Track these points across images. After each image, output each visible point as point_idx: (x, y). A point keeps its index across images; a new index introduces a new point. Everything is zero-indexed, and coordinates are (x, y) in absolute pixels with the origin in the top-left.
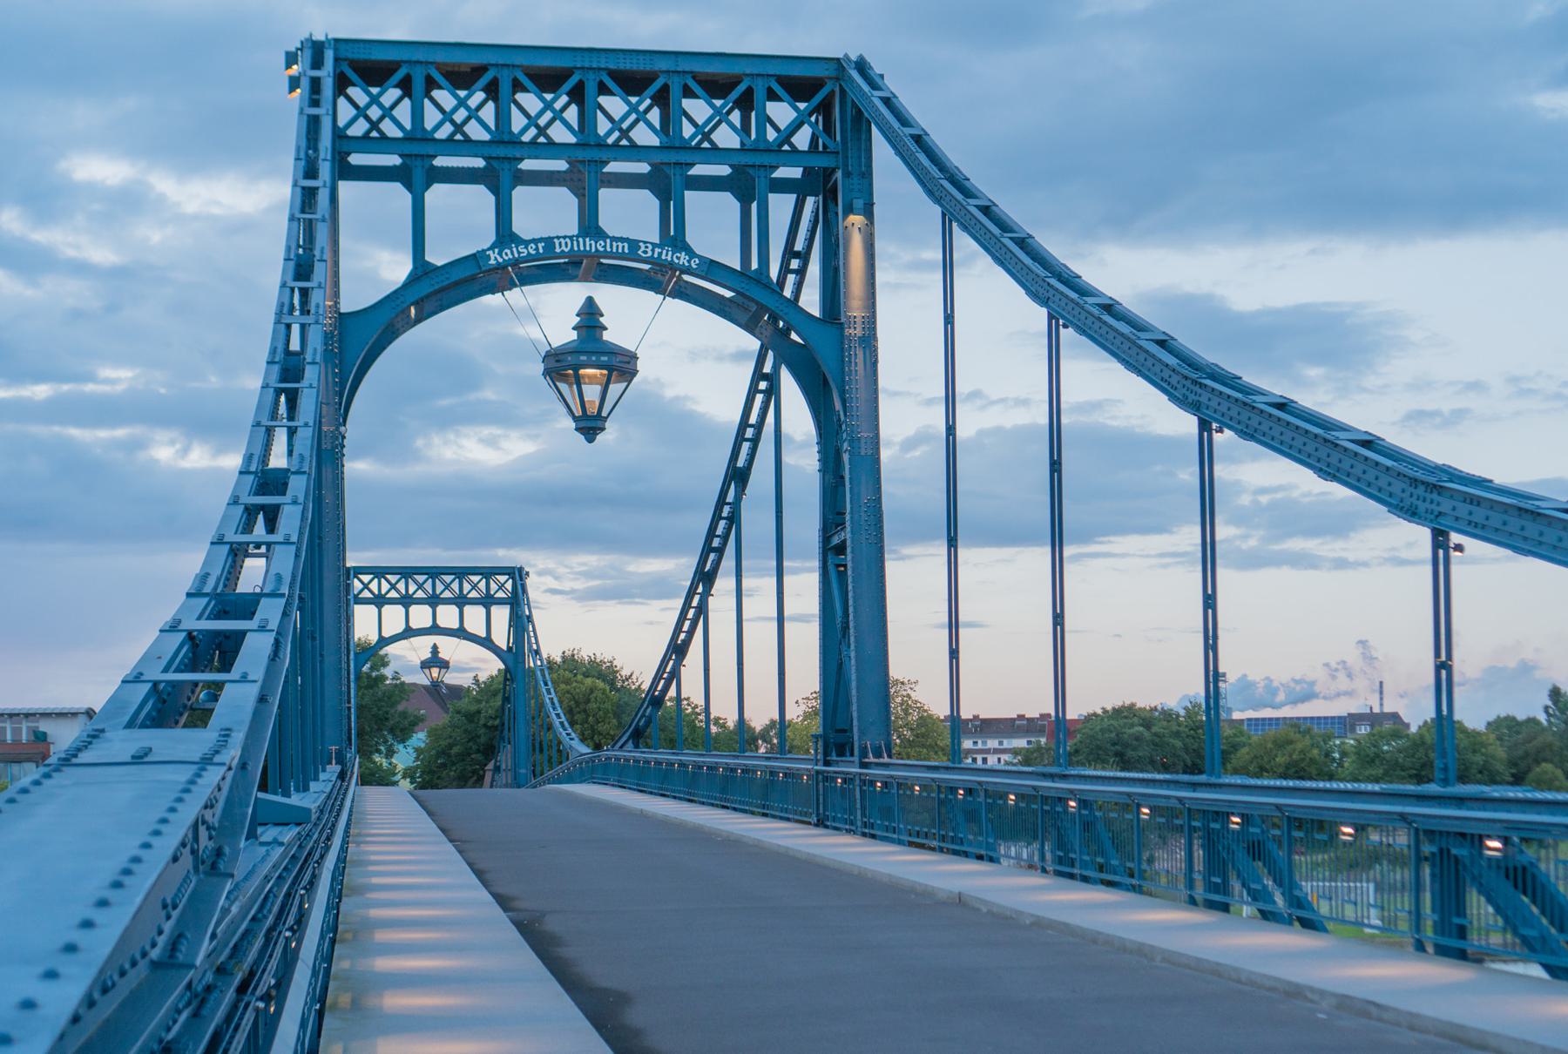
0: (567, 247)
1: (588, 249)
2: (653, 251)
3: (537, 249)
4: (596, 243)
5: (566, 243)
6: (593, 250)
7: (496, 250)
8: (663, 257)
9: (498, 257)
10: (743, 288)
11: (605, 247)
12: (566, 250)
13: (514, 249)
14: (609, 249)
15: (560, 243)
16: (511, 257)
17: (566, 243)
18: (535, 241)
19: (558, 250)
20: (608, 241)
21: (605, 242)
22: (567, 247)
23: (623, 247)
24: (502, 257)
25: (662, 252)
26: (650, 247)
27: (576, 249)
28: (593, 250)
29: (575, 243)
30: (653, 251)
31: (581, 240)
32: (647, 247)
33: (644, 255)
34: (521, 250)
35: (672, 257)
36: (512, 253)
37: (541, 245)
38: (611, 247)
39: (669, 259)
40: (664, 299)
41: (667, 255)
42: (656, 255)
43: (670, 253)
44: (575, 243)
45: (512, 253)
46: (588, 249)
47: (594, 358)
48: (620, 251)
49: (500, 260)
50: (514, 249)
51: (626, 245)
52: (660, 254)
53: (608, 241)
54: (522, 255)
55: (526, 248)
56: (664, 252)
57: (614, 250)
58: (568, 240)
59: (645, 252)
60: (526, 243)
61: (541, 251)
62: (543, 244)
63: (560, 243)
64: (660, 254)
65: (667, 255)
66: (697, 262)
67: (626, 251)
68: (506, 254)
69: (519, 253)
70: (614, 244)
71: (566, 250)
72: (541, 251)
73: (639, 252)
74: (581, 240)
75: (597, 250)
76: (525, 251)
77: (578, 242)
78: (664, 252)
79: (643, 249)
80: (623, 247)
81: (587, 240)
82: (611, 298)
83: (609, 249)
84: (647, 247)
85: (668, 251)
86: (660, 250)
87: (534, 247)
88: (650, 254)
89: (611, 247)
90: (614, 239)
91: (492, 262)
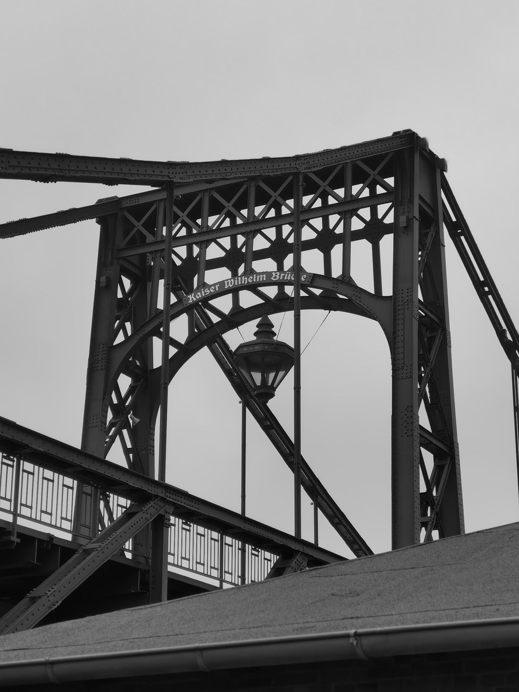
0: (231, 284)
1: (243, 283)
2: (280, 276)
4: (248, 278)
5: (231, 282)
7: (193, 294)
8: (286, 278)
9: (194, 298)
10: (334, 287)
11: (253, 279)
12: (231, 286)
13: (203, 292)
15: (228, 283)
16: (200, 296)
17: (231, 282)
18: (214, 285)
19: (226, 287)
20: (255, 275)
21: (253, 277)
22: (231, 284)
23: (263, 277)
24: (195, 297)
25: (285, 276)
27: (236, 284)
28: (246, 283)
29: (236, 281)
30: (280, 276)
32: (276, 275)
33: (274, 280)
34: (206, 291)
35: (291, 277)
36: (201, 294)
37: (217, 286)
38: (256, 279)
40: (330, 312)
41: (287, 277)
42: (281, 278)
43: (290, 275)
44: (236, 281)
45: (201, 294)
46: (243, 283)
47: (251, 349)
48: (261, 280)
49: (195, 299)
50: (203, 292)
51: (265, 276)
52: (284, 277)
53: (255, 275)
54: (206, 294)
55: (209, 289)
56: (286, 275)
57: (258, 280)
59: (275, 278)
60: (209, 286)
61: (217, 289)
62: (218, 285)
63: (228, 283)
64: (284, 277)
65: (287, 277)
66: (305, 276)
67: (265, 279)
68: (198, 295)
69: (205, 293)
70: (258, 277)
71: (231, 286)
72: (217, 289)
73: (272, 279)
75: (248, 282)
76: (209, 291)
78: (286, 275)
79: (274, 276)
80: (263, 277)
81: (243, 277)
83: (255, 281)
84: (276, 275)
85: (288, 274)
86: (284, 275)
87: (213, 287)
89: (256, 279)
90: (260, 274)
91: (191, 301)
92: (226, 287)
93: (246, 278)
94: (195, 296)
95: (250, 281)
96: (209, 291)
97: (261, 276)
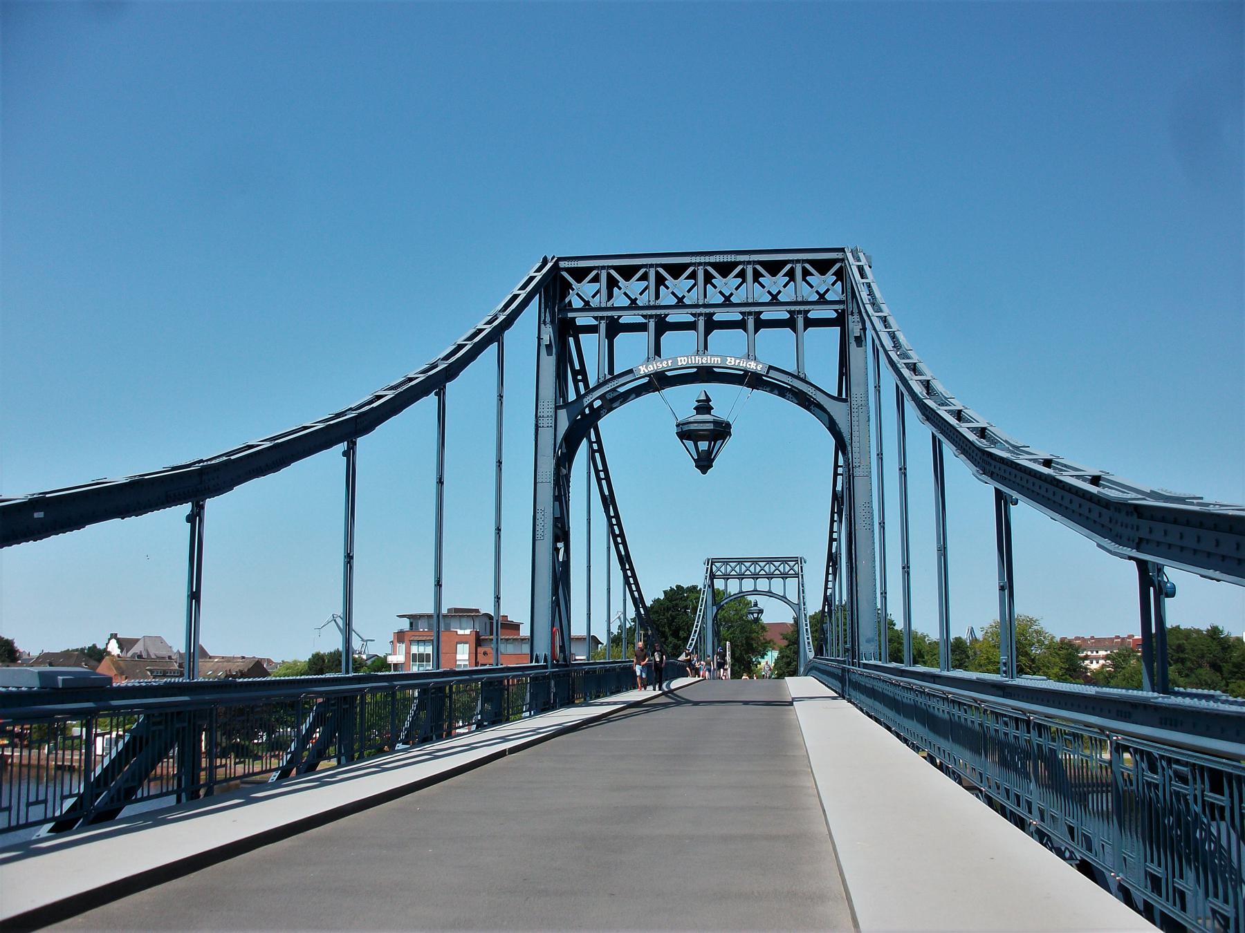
2: (735, 361)
3: (667, 364)
6: (700, 363)
7: (644, 366)
8: (741, 365)
11: (707, 360)
13: (655, 365)
14: (709, 362)
19: (680, 364)
26: (733, 359)
28: (700, 363)
29: (690, 360)
30: (735, 361)
31: (693, 357)
36: (654, 367)
37: (670, 362)
39: (744, 365)
43: (745, 363)
44: (690, 360)
45: (654, 367)
49: (647, 371)
50: (655, 365)
51: (719, 359)
53: (709, 357)
56: (742, 362)
58: (685, 358)
61: (670, 365)
70: (713, 359)
71: (685, 364)
72: (670, 365)
73: (727, 363)
74: (693, 357)
76: (661, 366)
77: (691, 359)
78: (742, 362)
82: (715, 391)
83: (709, 362)
88: (733, 364)
89: (711, 361)
91: (642, 372)
92: (680, 364)
93: (700, 359)
94: (646, 368)
95: (704, 362)
96: (661, 366)
97: (716, 359)
